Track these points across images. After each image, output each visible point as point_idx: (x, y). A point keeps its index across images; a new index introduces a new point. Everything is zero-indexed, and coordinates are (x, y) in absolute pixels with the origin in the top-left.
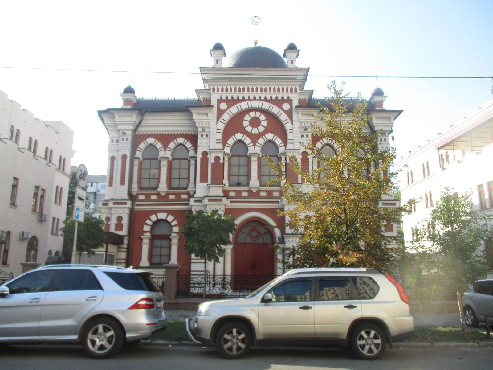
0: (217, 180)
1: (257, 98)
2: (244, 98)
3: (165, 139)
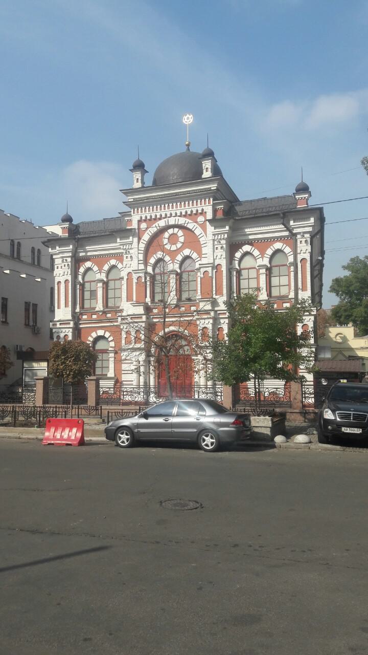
1: (174, 215)
3: (100, 260)
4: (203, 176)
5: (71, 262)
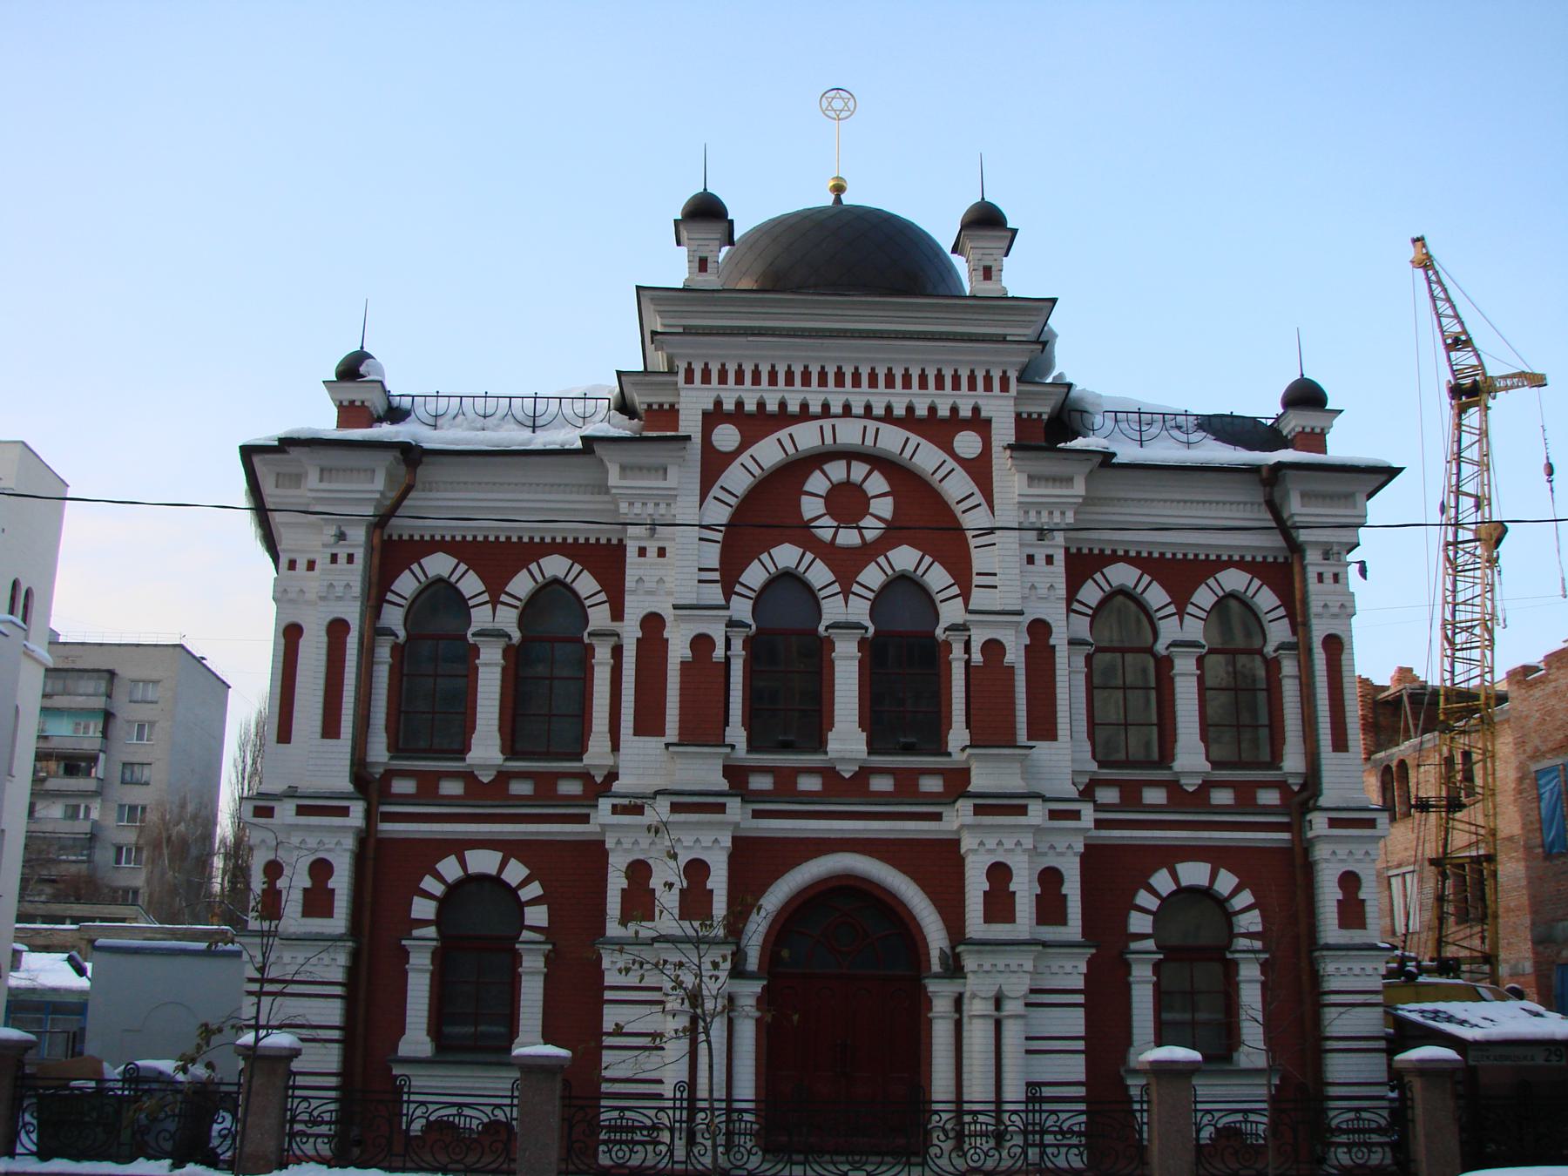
0: (702, 729)
1: (858, 409)
2: (804, 406)
3: (496, 559)
5: (370, 549)
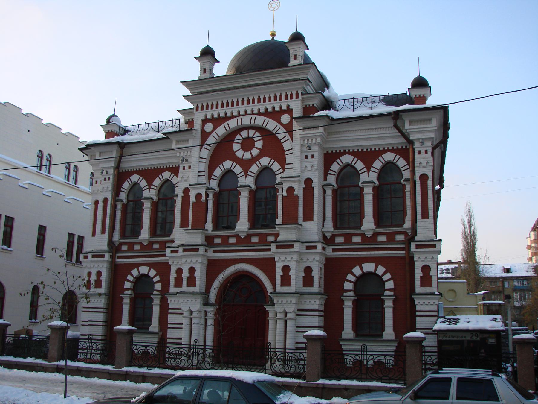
0: (199, 225)
1: (249, 112)
3: (149, 174)
4: (290, 64)
5: (114, 175)
